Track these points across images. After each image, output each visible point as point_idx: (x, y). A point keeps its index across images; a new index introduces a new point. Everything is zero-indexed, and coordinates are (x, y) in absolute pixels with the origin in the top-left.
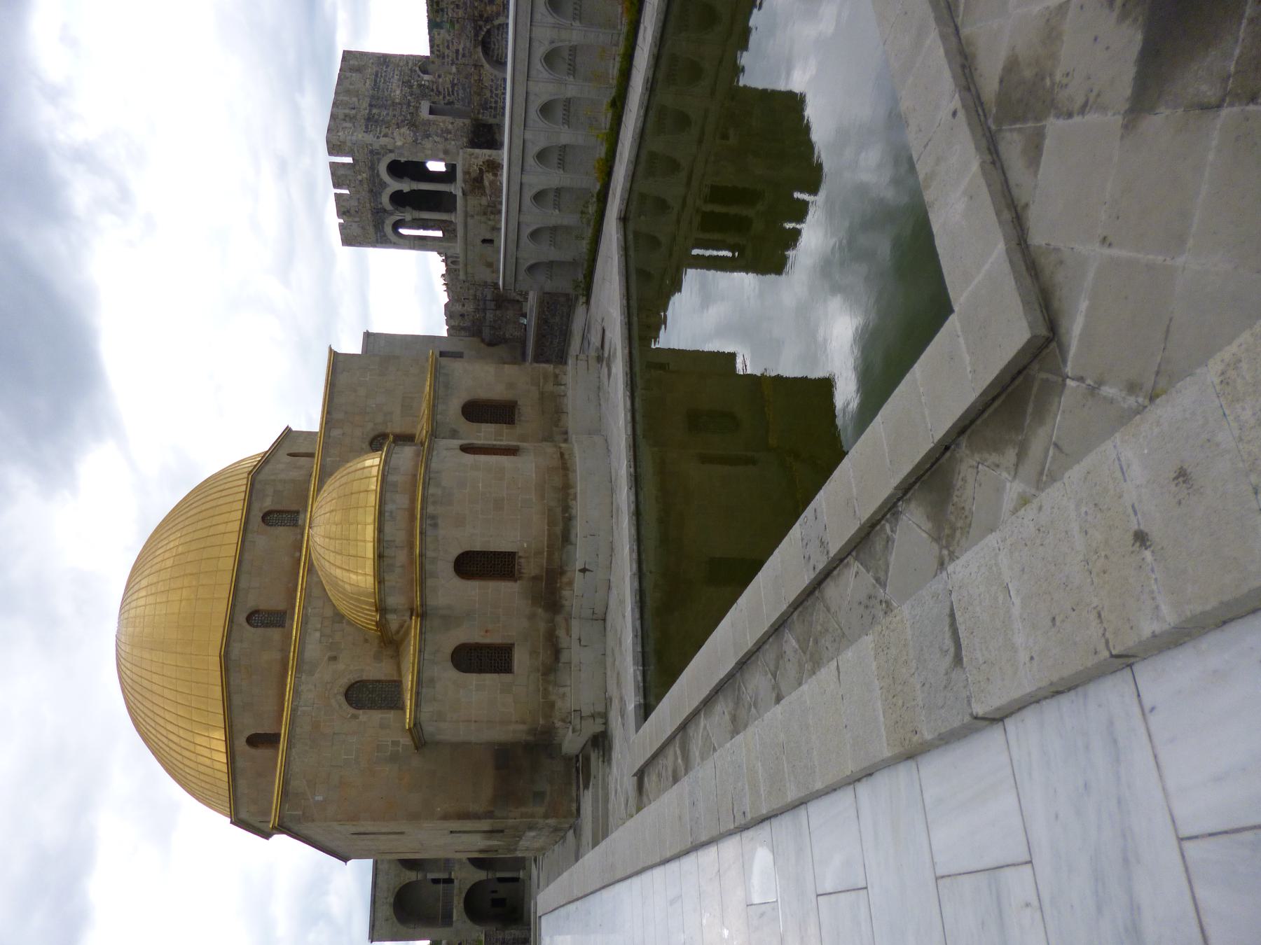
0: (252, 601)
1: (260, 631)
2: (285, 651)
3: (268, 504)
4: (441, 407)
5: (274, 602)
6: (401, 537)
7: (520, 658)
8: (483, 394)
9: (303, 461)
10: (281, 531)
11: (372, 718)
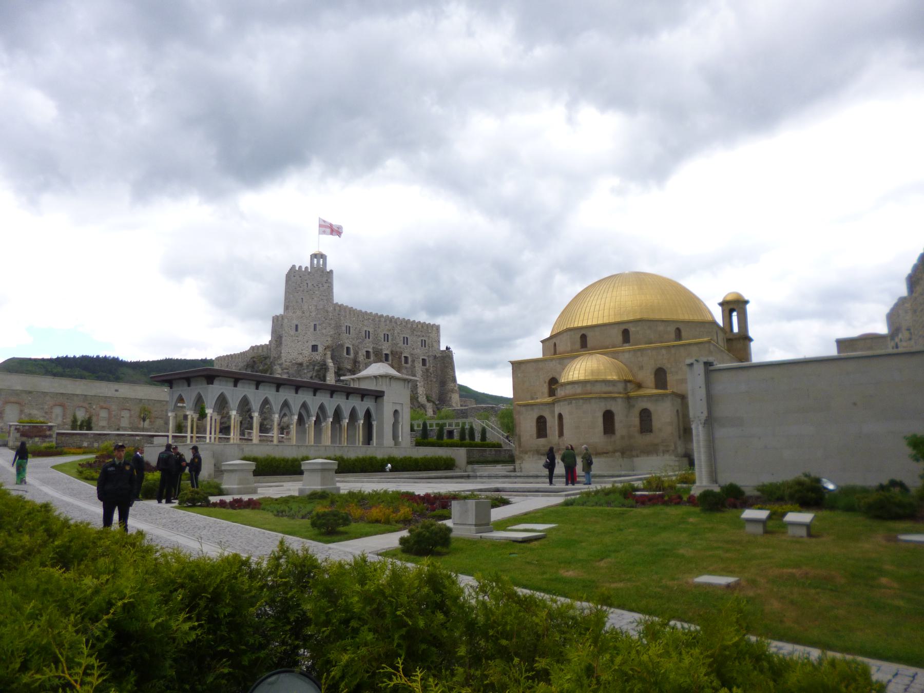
0: (590, 335)
1: (579, 340)
2: (572, 351)
3: (632, 329)
4: (645, 399)
5: (590, 343)
6: (567, 392)
7: (542, 441)
8: (654, 418)
9: (673, 336)
10: (620, 338)
11: (545, 389)
